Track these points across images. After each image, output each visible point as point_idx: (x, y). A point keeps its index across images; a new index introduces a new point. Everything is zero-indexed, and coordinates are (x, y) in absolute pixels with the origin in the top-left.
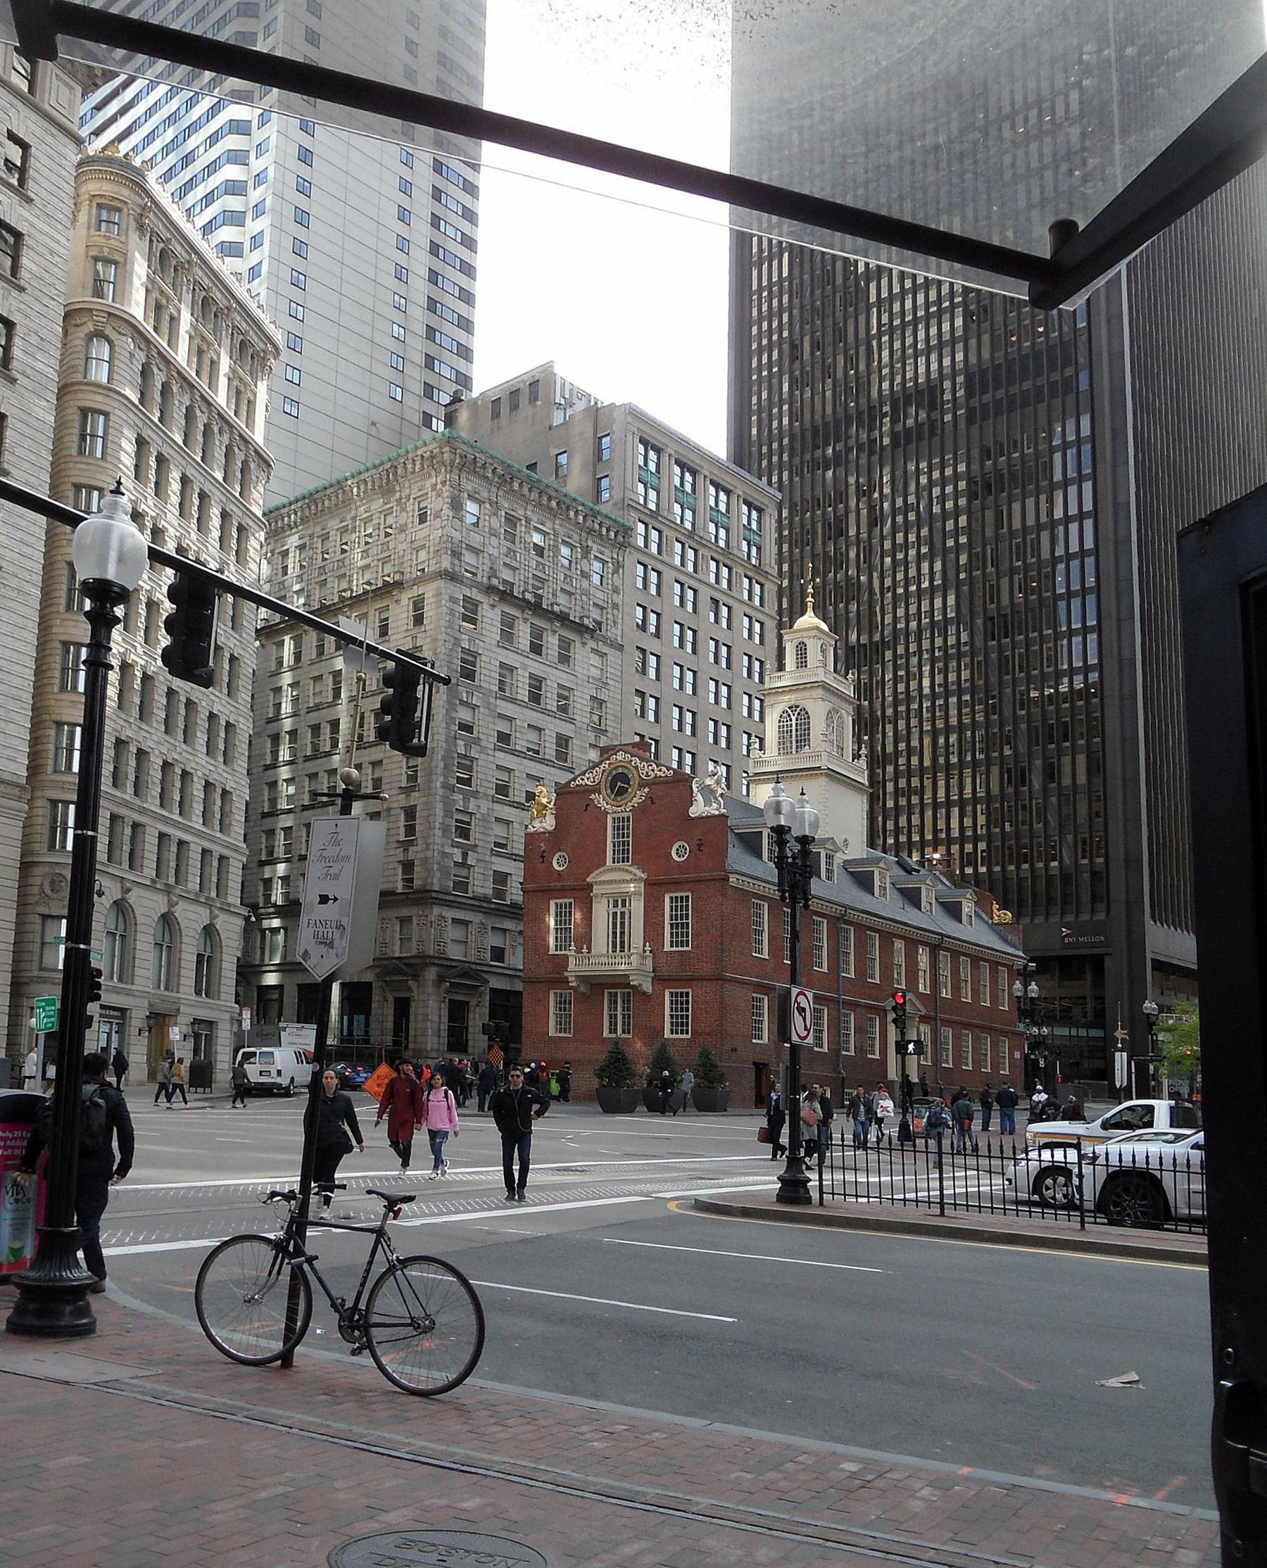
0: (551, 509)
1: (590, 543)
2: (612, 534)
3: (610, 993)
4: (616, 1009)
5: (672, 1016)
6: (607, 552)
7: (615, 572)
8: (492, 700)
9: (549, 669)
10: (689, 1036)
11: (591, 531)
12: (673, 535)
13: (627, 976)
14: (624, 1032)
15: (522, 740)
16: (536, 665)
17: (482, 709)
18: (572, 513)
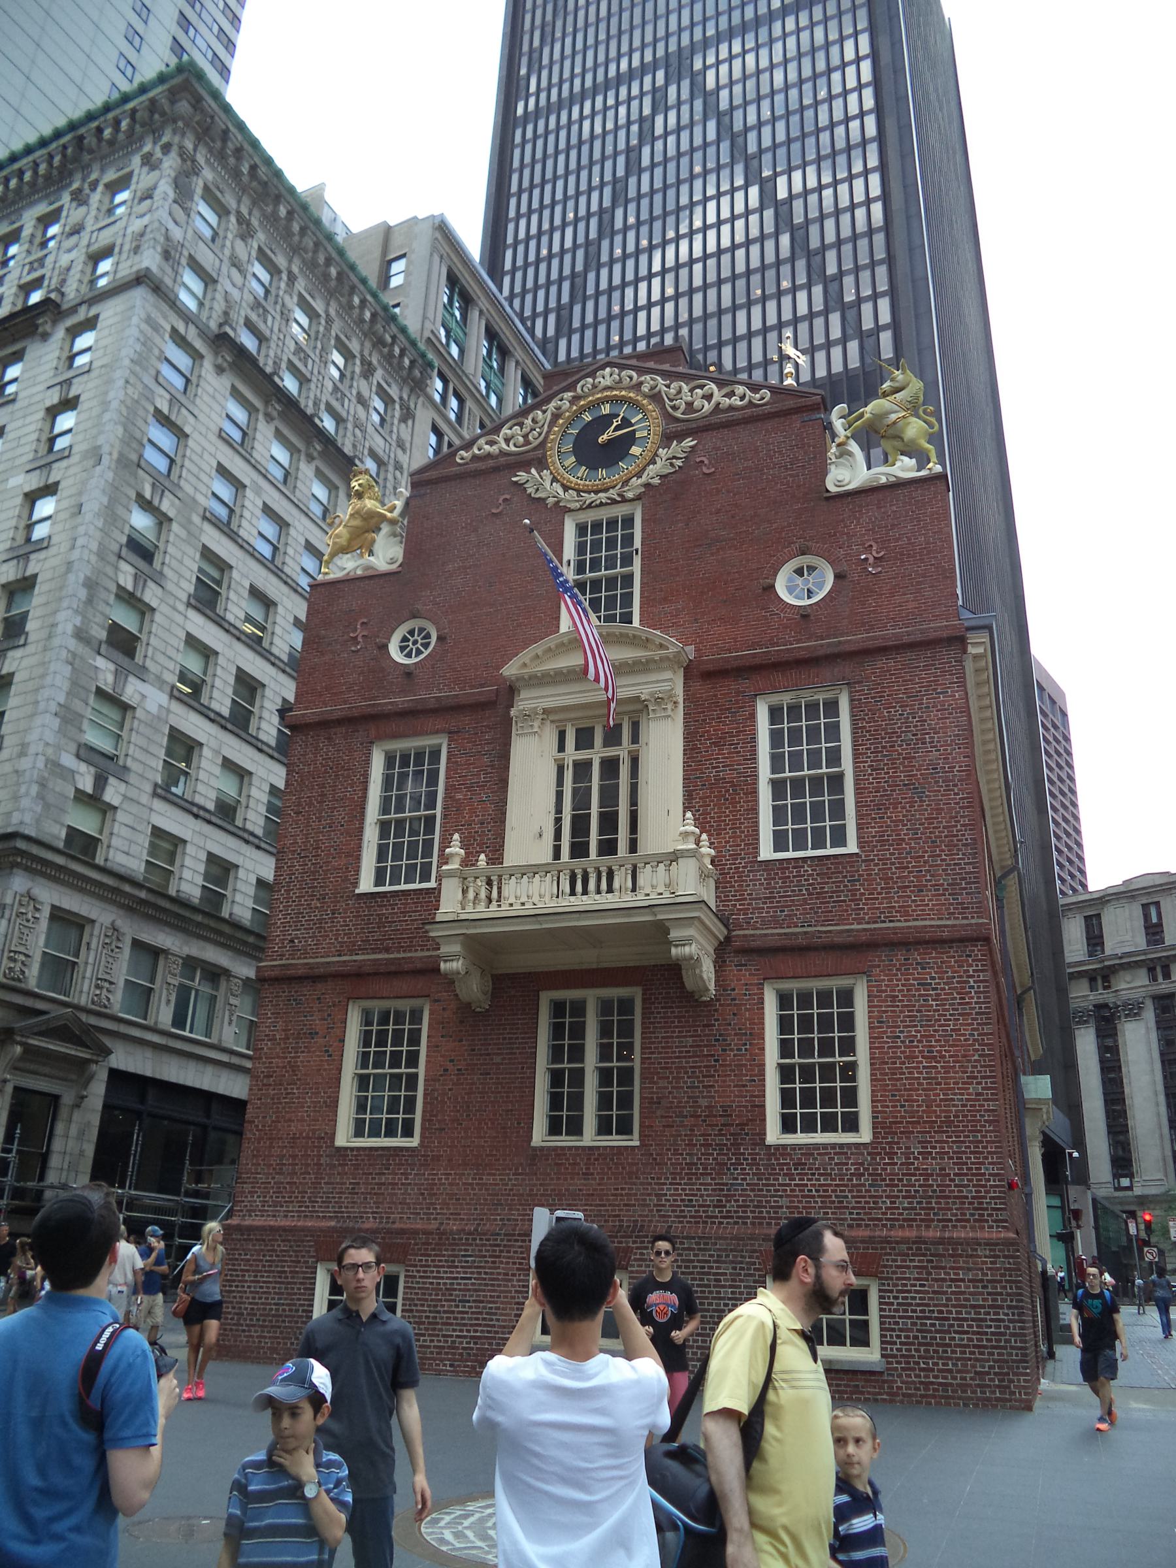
0: (326, 276)
1: (375, 362)
2: (407, 362)
3: (558, 1008)
4: (577, 1053)
5: (786, 1073)
6: (394, 386)
7: (404, 420)
8: (196, 519)
9: (295, 511)
10: (865, 1135)
11: (379, 343)
12: (477, 413)
13: (661, 929)
14: (604, 1128)
15: (237, 607)
16: (276, 495)
17: (175, 527)
18: (356, 300)
